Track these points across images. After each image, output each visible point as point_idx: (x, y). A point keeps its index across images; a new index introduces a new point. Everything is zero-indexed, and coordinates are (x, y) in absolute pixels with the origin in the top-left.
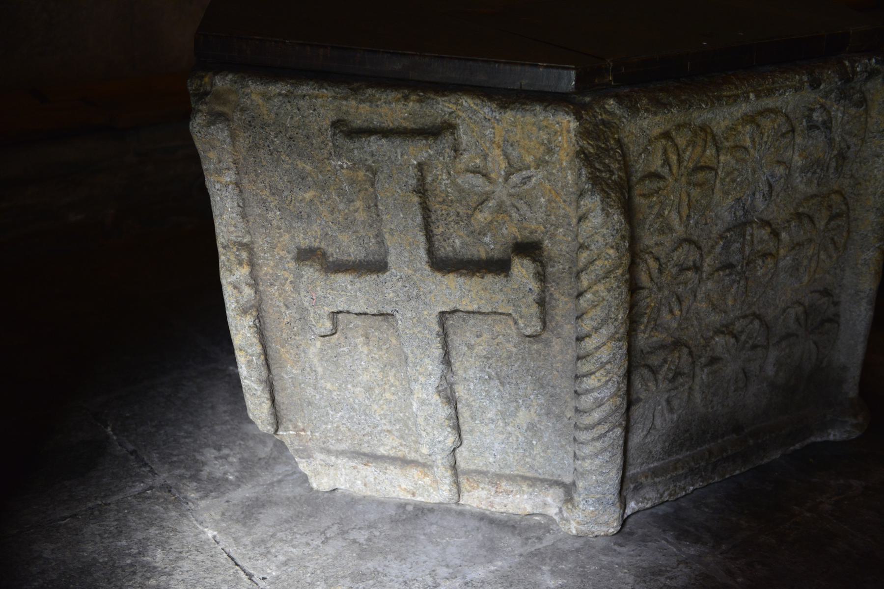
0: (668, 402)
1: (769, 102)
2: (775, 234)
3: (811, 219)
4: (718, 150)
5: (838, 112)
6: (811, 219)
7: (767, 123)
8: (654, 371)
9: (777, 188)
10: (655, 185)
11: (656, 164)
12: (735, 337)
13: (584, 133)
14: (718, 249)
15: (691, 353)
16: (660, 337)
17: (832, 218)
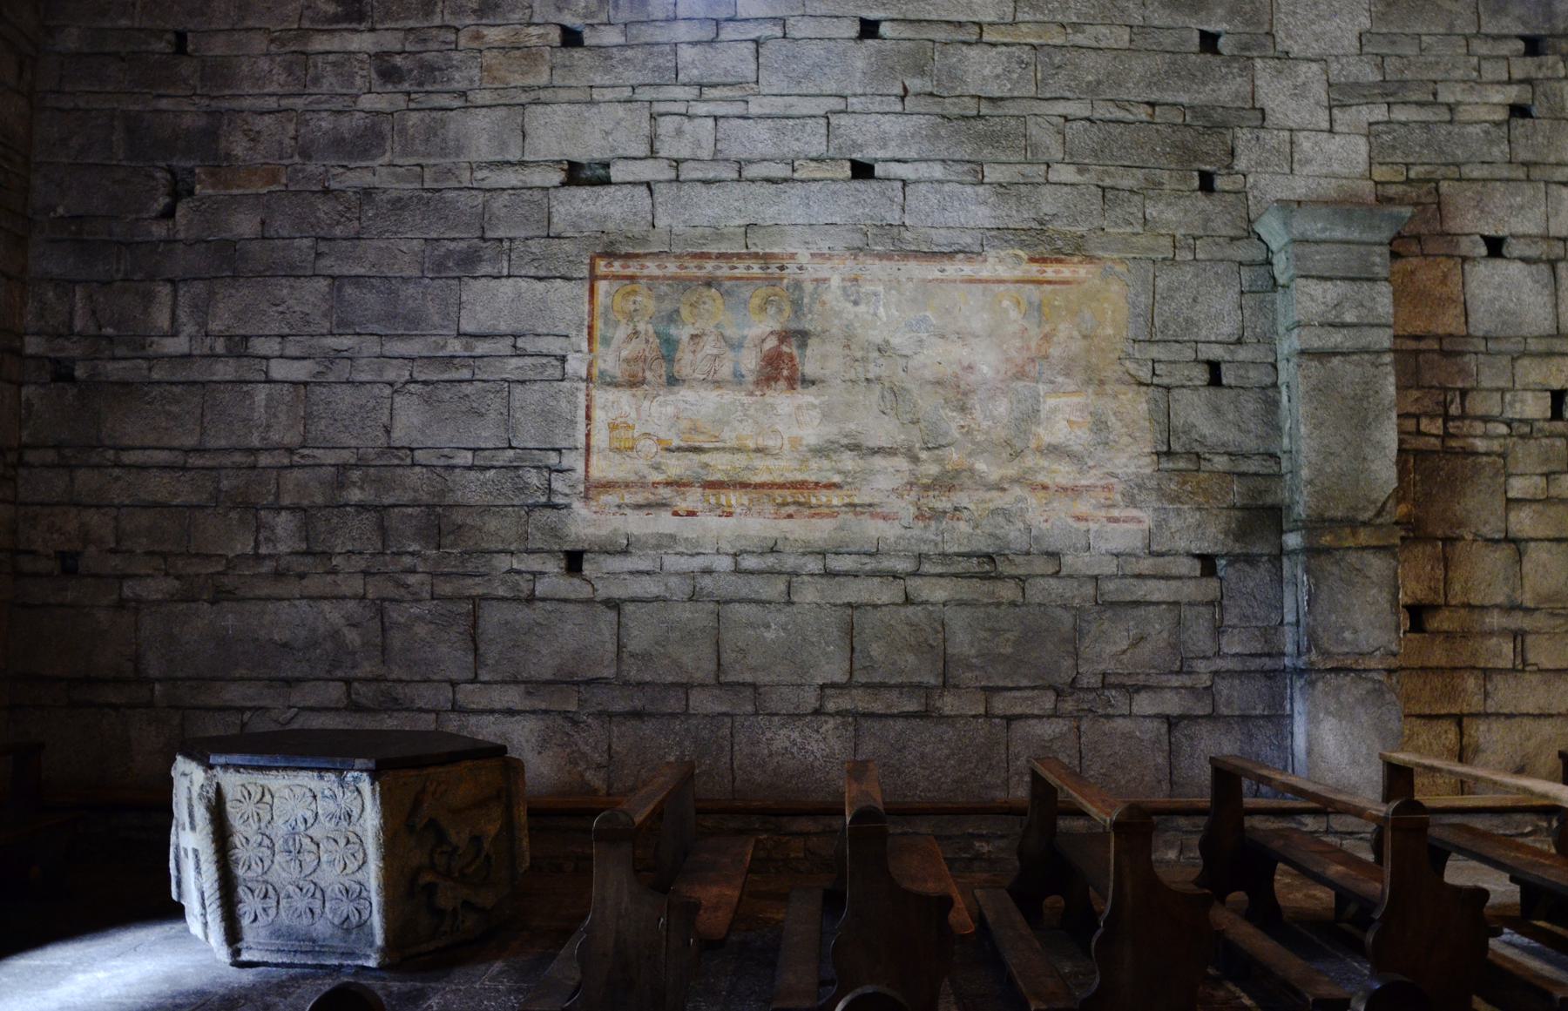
0: (264, 910)
1: (297, 781)
2: (318, 845)
3: (336, 841)
4: (272, 797)
5: (339, 792)
6: (336, 841)
7: (298, 791)
8: (252, 891)
9: (310, 821)
10: (239, 804)
11: (239, 796)
12: (301, 890)
13: (207, 778)
14: (281, 842)
15: (274, 889)
16: (250, 874)
17: (348, 842)
